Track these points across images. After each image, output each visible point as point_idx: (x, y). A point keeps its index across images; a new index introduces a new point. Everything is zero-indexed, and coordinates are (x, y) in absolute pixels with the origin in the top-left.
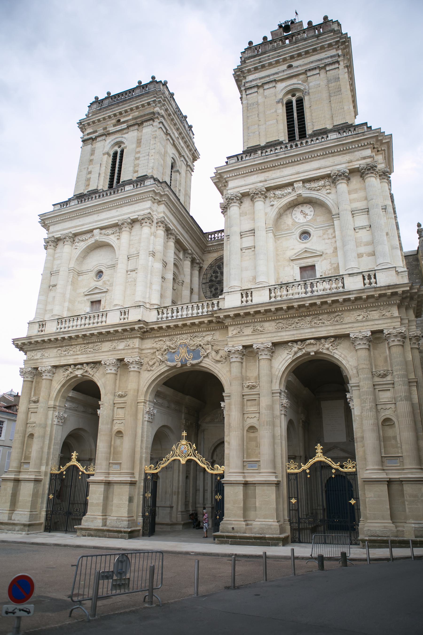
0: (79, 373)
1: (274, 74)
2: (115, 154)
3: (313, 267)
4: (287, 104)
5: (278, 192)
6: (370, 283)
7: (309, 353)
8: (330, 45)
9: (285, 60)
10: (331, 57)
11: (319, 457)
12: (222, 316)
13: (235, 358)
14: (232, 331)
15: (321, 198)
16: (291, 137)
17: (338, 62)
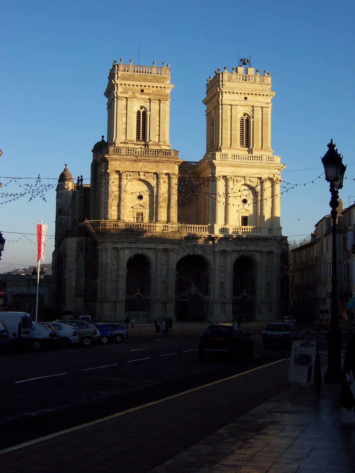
0: (140, 252)
2: (139, 112)
5: (239, 179)
11: (244, 294)
13: (218, 255)
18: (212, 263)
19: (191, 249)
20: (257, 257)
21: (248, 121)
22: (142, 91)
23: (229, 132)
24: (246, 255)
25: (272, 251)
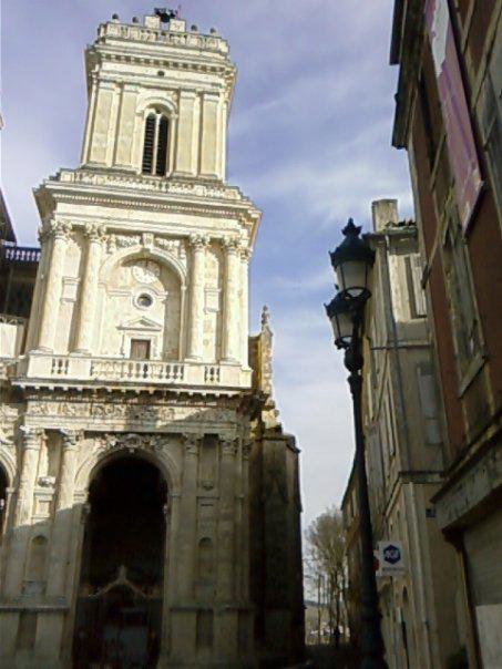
1: (139, 75)
3: (148, 343)
4: (148, 119)
6: (212, 379)
7: (127, 449)
8: (213, 69)
9: (157, 63)
10: (213, 84)
11: (122, 578)
14: (33, 406)
15: (173, 262)
16: (147, 169)
17: (218, 94)
18: (11, 475)
20: (169, 456)
21: (165, 124)
23: (111, 139)
24: (132, 447)
25: (216, 435)
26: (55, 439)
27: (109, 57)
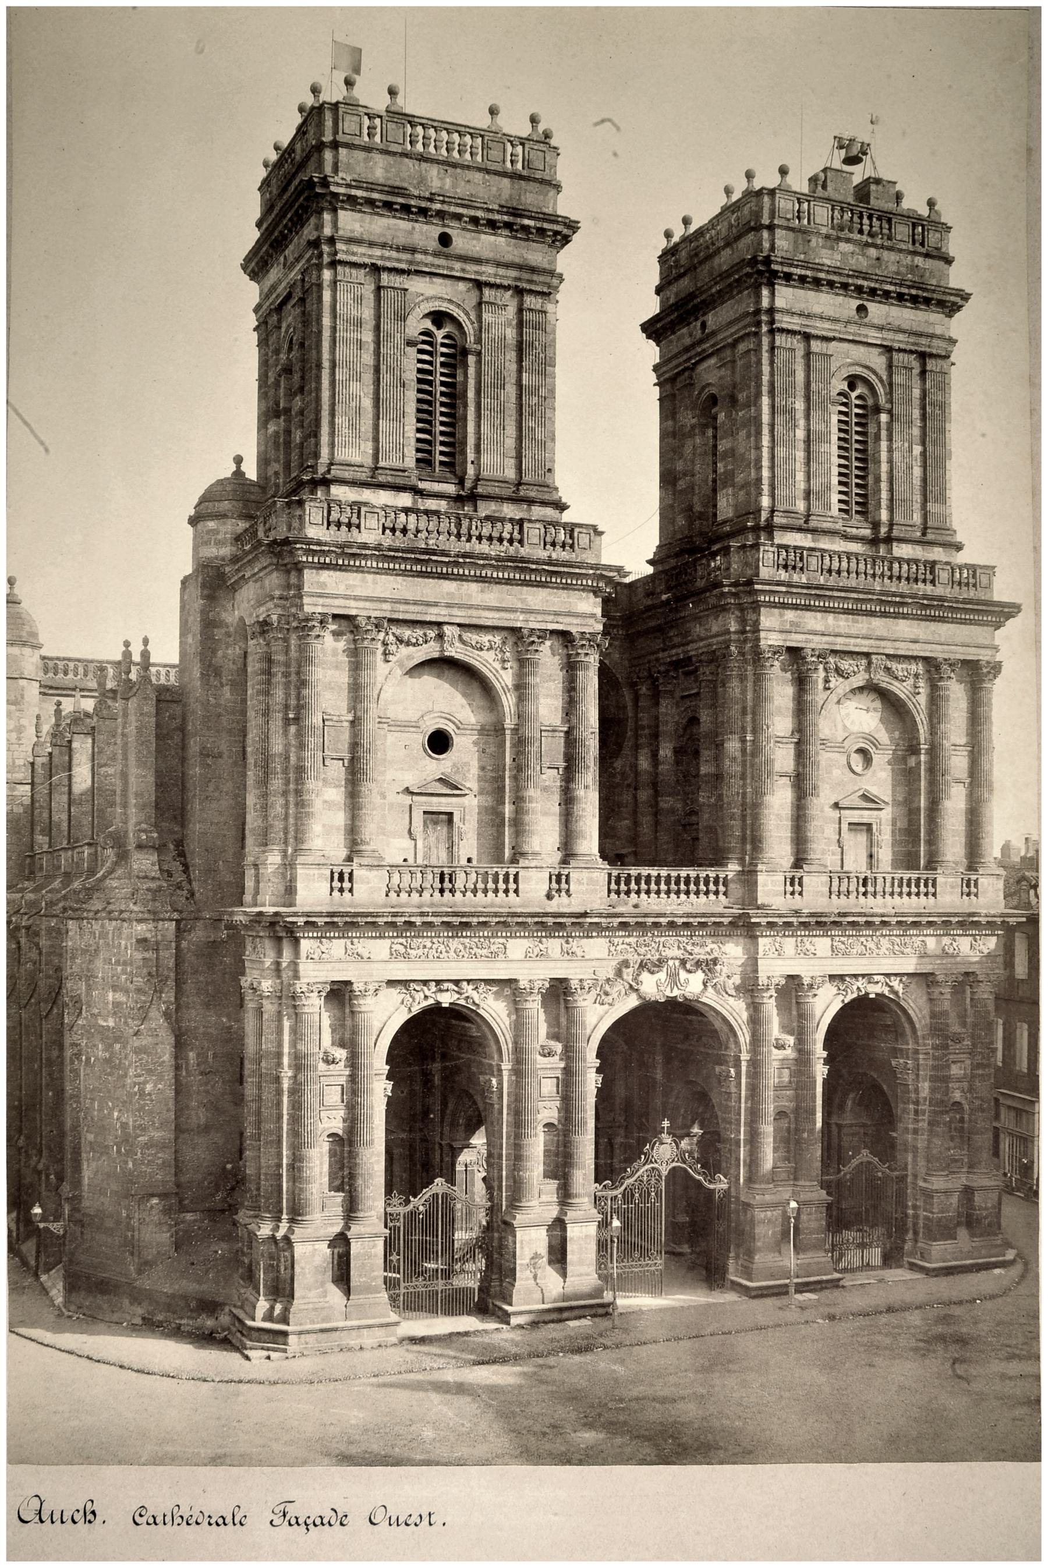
0: (446, 999)
3: (869, 826)
7: (867, 994)
12: (763, 921)
18: (744, 1037)
19: (662, 975)
22: (445, 240)
26: (793, 989)
27: (788, 277)
